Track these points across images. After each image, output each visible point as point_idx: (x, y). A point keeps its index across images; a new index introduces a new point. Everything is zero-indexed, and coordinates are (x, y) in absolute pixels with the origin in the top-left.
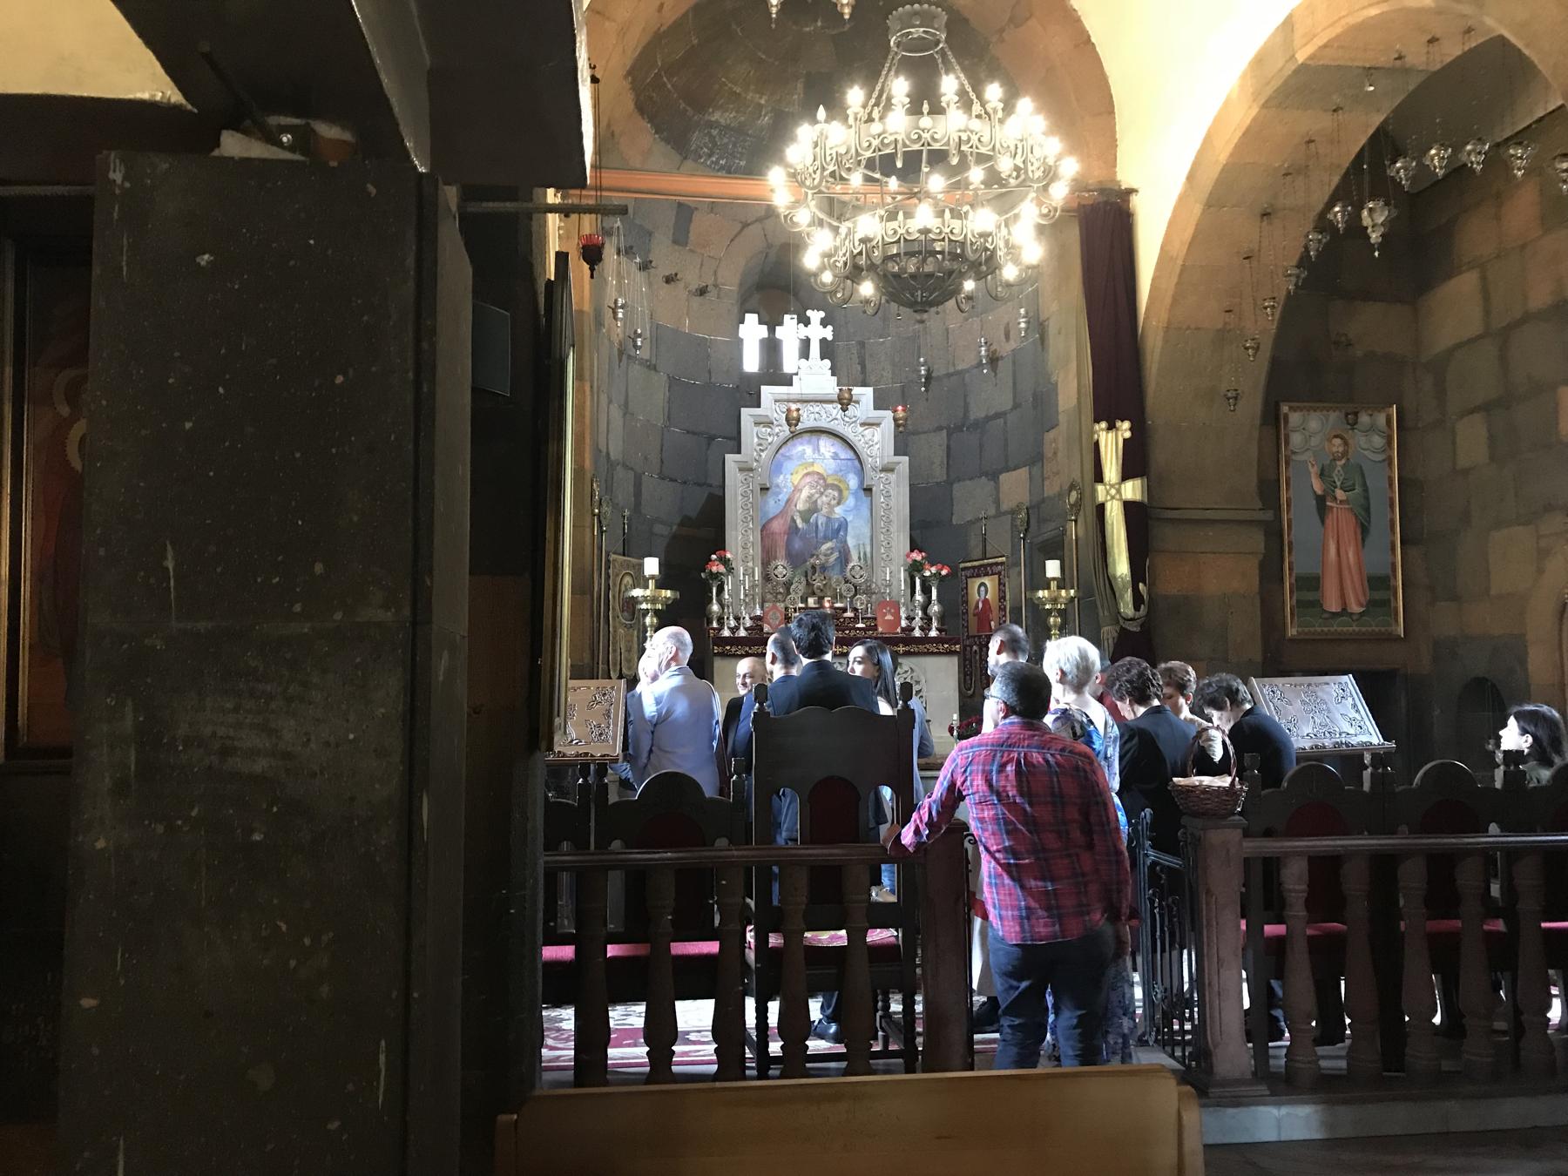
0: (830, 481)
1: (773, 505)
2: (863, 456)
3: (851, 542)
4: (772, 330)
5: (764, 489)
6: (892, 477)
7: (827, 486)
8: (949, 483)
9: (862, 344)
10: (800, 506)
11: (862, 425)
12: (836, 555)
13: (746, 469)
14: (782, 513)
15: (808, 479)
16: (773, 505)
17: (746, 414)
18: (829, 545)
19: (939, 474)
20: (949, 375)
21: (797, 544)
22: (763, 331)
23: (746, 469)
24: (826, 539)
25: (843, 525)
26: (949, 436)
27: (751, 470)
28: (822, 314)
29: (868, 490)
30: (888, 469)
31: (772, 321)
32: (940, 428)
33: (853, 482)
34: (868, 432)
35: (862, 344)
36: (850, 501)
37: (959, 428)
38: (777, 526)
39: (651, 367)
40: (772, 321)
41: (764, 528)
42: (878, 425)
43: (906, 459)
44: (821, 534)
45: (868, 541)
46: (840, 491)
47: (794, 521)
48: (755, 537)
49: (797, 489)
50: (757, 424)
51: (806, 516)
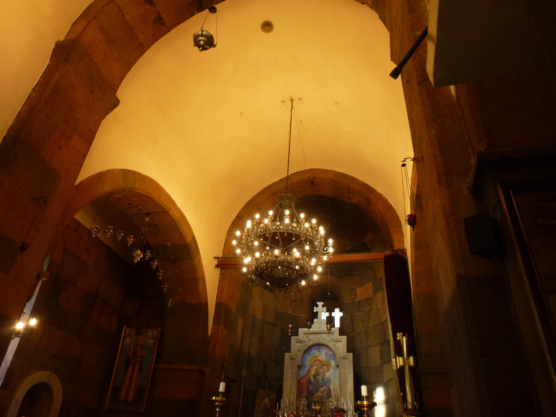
0: (324, 363)
1: (303, 373)
2: (336, 353)
3: (332, 387)
4: (330, 314)
5: (299, 367)
6: (347, 361)
7: (323, 365)
8: (382, 365)
9: (352, 315)
10: (313, 373)
11: (335, 341)
12: (326, 392)
13: (292, 359)
14: (306, 375)
15: (316, 363)
16: (303, 373)
17: (293, 338)
18: (323, 388)
19: (378, 362)
20: (379, 324)
21: (311, 388)
22: (327, 314)
23: (292, 359)
24: (322, 386)
25: (329, 380)
26: (381, 346)
27: (294, 359)
28: (323, 303)
29: (338, 366)
30: (344, 358)
31: (330, 310)
32: (378, 344)
33: (333, 363)
34: (338, 344)
35: (352, 315)
36: (332, 371)
37: (383, 344)
38: (303, 381)
39: (274, 325)
40: (330, 310)
41: (298, 383)
42: (341, 341)
43: (352, 354)
44: (320, 384)
45: (338, 387)
46: (328, 368)
47: (310, 379)
48: (295, 385)
49: (312, 366)
50: (297, 342)
51: (315, 376)
